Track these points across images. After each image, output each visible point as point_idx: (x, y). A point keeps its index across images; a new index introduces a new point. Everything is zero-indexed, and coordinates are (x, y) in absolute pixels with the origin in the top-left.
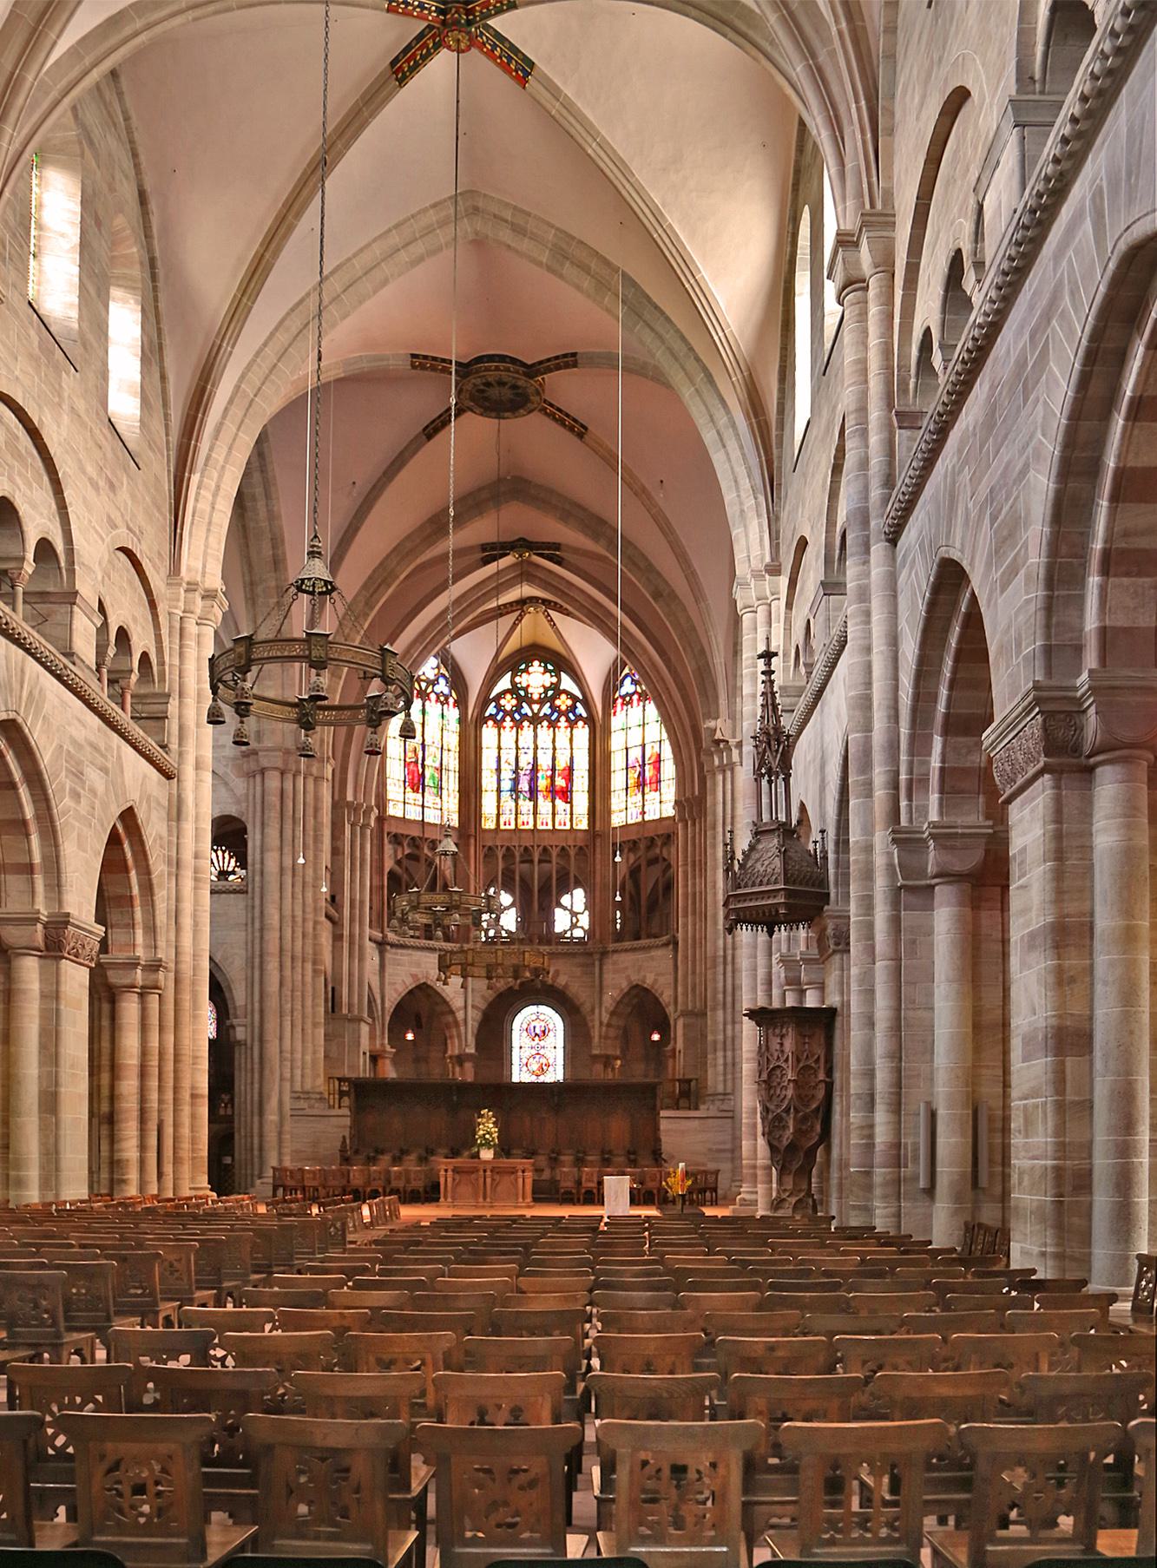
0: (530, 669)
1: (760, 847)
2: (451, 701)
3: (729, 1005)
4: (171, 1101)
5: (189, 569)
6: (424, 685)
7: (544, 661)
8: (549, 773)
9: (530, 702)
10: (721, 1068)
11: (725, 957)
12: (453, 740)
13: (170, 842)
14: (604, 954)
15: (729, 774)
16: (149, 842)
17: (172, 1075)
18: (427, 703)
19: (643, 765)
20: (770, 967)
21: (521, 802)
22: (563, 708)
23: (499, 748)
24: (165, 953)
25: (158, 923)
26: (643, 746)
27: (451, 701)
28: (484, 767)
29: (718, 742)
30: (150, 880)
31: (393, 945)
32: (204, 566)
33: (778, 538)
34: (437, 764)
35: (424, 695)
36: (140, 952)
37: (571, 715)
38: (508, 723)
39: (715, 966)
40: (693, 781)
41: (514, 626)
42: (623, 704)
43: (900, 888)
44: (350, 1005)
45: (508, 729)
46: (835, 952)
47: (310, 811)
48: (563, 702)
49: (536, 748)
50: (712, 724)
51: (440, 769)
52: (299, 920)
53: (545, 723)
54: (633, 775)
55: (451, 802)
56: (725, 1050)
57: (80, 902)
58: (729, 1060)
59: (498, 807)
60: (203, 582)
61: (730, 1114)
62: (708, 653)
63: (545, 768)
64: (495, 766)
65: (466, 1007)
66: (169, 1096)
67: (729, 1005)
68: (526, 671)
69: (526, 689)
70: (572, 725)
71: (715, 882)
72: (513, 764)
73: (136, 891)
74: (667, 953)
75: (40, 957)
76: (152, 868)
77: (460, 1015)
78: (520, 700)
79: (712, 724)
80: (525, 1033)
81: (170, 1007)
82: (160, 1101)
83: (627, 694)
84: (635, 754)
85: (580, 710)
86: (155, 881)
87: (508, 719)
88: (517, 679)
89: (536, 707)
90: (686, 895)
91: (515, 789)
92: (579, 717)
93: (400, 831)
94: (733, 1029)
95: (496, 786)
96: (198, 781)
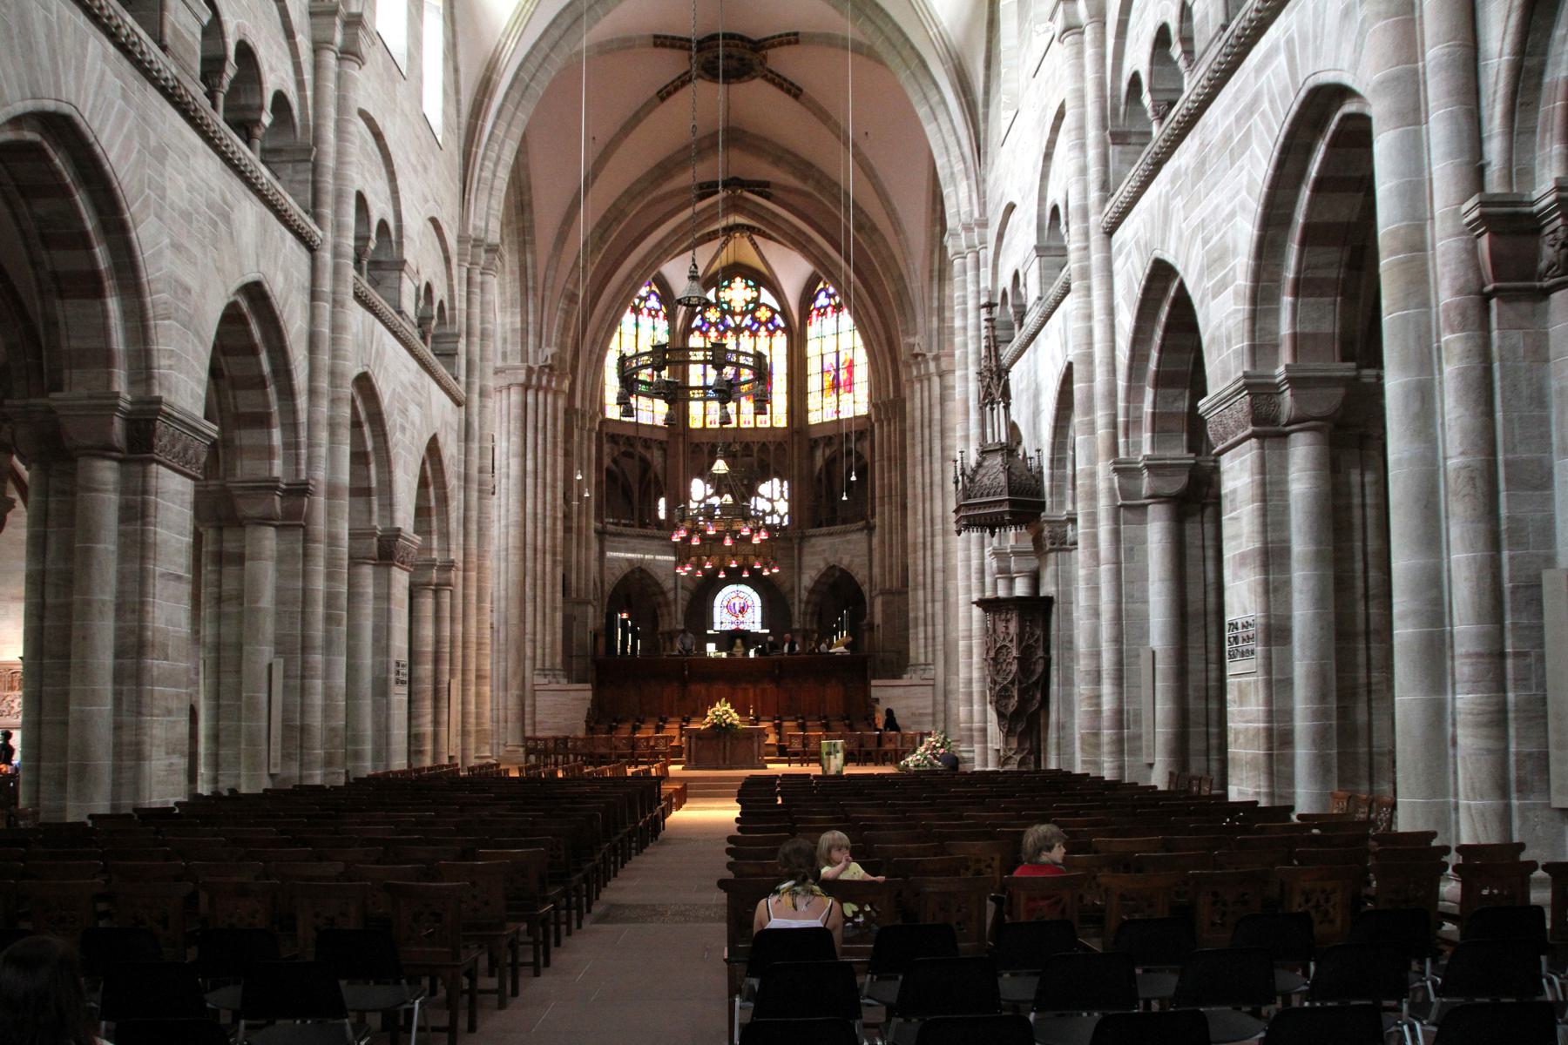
5: (475, 228)
10: (922, 642)
14: (803, 538)
15: (926, 383)
16: (446, 461)
25: (451, 530)
29: (916, 356)
30: (445, 493)
32: (487, 225)
39: (915, 551)
40: (888, 386)
44: (578, 590)
50: (911, 340)
52: (540, 516)
56: (925, 625)
60: (486, 237)
62: (906, 277)
65: (676, 588)
67: (929, 586)
74: (860, 537)
79: (911, 340)
81: (459, 601)
90: (882, 487)
93: (616, 432)
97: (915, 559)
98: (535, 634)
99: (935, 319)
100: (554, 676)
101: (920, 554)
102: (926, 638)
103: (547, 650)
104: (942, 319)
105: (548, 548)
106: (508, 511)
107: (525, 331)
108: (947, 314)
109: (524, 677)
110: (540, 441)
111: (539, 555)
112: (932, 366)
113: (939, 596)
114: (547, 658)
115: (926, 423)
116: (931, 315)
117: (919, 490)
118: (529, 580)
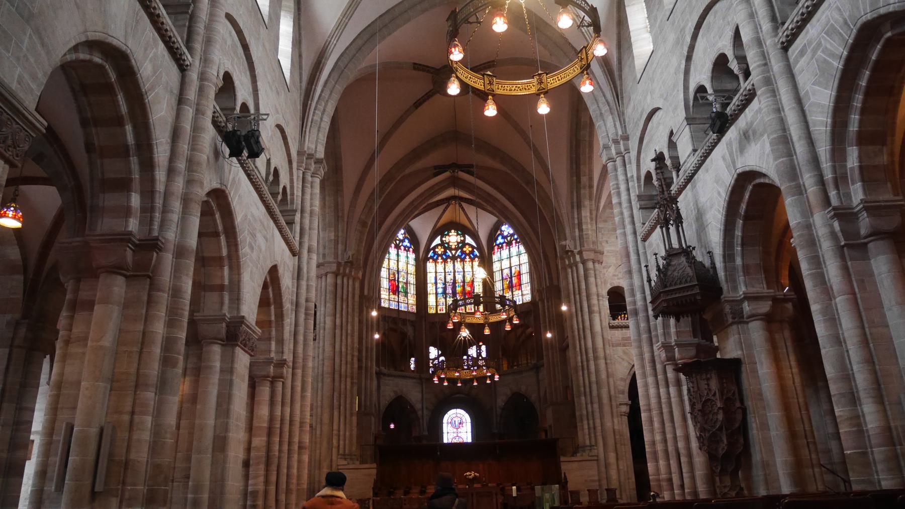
0: (450, 234)
1: (673, 263)
2: (411, 249)
3: (588, 393)
4: (286, 451)
6: (398, 242)
7: (457, 230)
8: (462, 284)
9: (451, 249)
10: (586, 431)
11: (583, 366)
12: (412, 269)
13: (293, 291)
15: (574, 268)
17: (288, 434)
18: (400, 250)
19: (511, 278)
20: (652, 352)
21: (448, 299)
22: (468, 252)
23: (436, 272)
24: (288, 356)
26: (511, 268)
27: (411, 249)
28: (428, 282)
29: (568, 252)
31: (385, 375)
33: (625, 123)
34: (405, 281)
35: (398, 247)
36: (273, 355)
37: (471, 255)
38: (440, 260)
39: (577, 372)
41: (444, 211)
42: (498, 249)
43: (843, 247)
45: (440, 263)
46: (733, 323)
47: (350, 295)
48: (467, 249)
49: (454, 272)
50: (564, 243)
51: (406, 283)
52: (344, 354)
53: (459, 260)
54: (507, 283)
55: (412, 300)
56: (588, 419)
57: (249, 309)
58: (591, 425)
59: (437, 302)
61: (596, 458)
63: (460, 281)
64: (433, 281)
66: (285, 447)
67: (588, 393)
68: (448, 235)
69: (448, 243)
70: (472, 260)
71: (572, 327)
72: (443, 280)
73: (273, 318)
75: (222, 345)
76: (284, 304)
77: (420, 413)
78: (445, 249)
79: (564, 243)
80: (450, 425)
82: (280, 451)
83: (500, 243)
84: (507, 272)
85: (476, 252)
86: (285, 312)
87: (440, 258)
88: (444, 239)
89: (454, 252)
91: (444, 293)
92: (476, 256)
94: (592, 407)
95: (434, 292)
96: (309, 259)
97: (577, 376)
98: (339, 431)
99: (577, 230)
100: (351, 459)
101: (580, 373)
102: (589, 429)
103: (347, 442)
104: (581, 230)
105: (348, 374)
106: (324, 350)
107: (336, 242)
108: (584, 227)
109: (331, 460)
110: (344, 307)
111: (343, 379)
112: (578, 258)
113: (596, 400)
114: (347, 447)
115: (577, 292)
116: (574, 228)
117: (576, 333)
118: (336, 394)
